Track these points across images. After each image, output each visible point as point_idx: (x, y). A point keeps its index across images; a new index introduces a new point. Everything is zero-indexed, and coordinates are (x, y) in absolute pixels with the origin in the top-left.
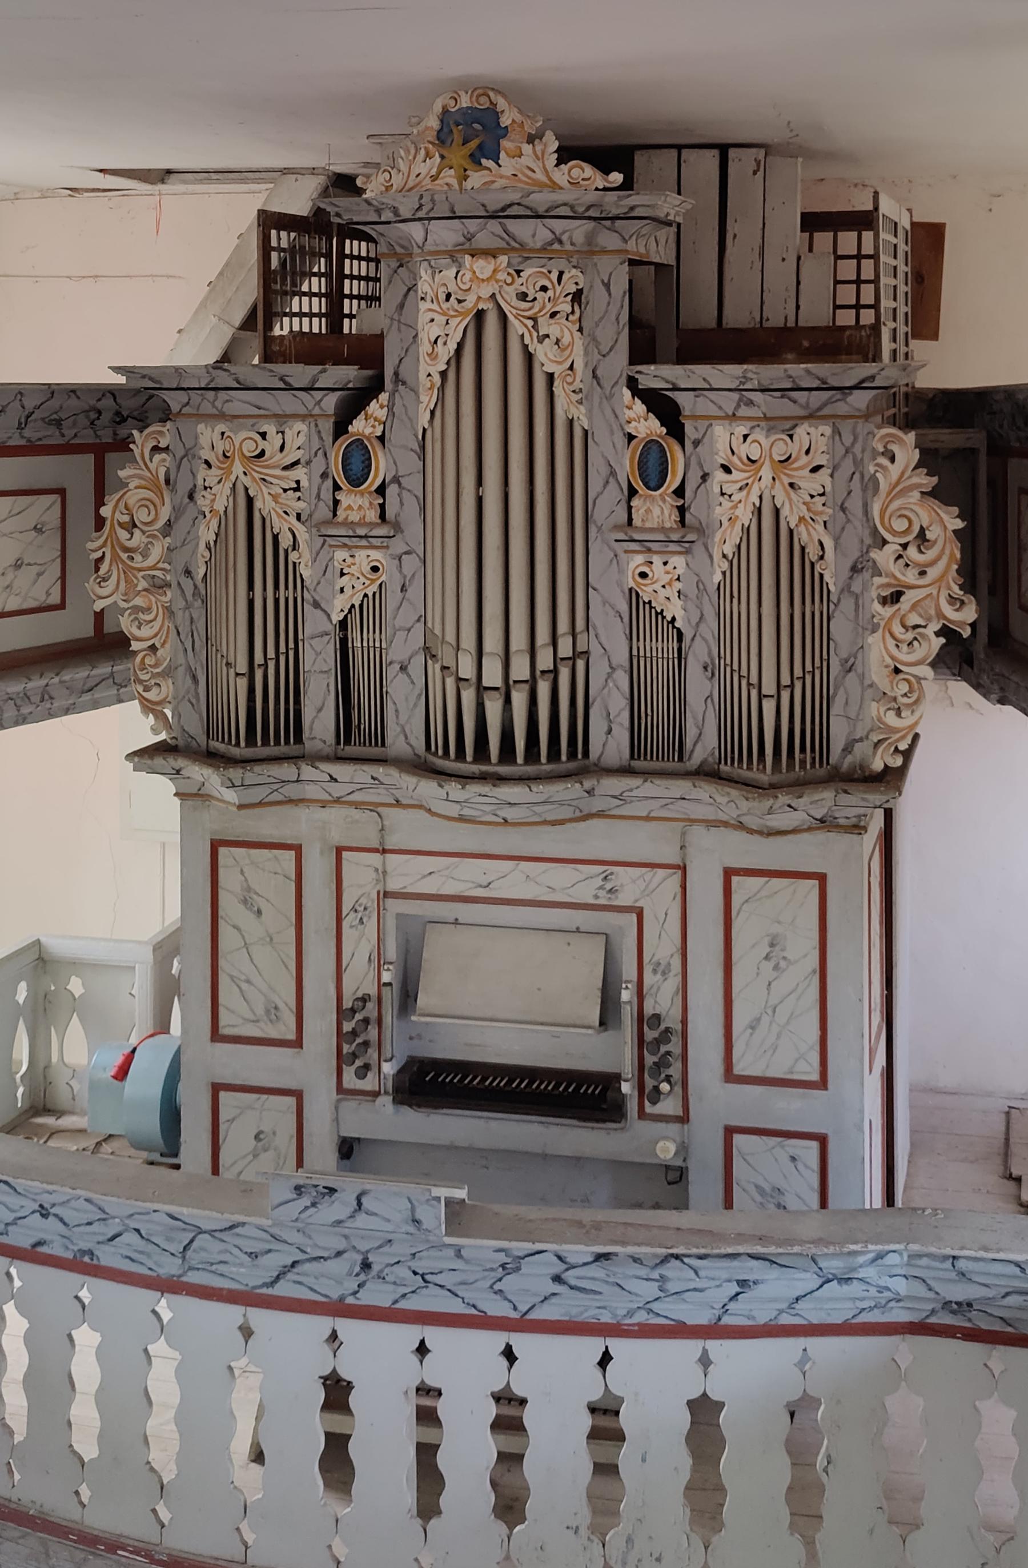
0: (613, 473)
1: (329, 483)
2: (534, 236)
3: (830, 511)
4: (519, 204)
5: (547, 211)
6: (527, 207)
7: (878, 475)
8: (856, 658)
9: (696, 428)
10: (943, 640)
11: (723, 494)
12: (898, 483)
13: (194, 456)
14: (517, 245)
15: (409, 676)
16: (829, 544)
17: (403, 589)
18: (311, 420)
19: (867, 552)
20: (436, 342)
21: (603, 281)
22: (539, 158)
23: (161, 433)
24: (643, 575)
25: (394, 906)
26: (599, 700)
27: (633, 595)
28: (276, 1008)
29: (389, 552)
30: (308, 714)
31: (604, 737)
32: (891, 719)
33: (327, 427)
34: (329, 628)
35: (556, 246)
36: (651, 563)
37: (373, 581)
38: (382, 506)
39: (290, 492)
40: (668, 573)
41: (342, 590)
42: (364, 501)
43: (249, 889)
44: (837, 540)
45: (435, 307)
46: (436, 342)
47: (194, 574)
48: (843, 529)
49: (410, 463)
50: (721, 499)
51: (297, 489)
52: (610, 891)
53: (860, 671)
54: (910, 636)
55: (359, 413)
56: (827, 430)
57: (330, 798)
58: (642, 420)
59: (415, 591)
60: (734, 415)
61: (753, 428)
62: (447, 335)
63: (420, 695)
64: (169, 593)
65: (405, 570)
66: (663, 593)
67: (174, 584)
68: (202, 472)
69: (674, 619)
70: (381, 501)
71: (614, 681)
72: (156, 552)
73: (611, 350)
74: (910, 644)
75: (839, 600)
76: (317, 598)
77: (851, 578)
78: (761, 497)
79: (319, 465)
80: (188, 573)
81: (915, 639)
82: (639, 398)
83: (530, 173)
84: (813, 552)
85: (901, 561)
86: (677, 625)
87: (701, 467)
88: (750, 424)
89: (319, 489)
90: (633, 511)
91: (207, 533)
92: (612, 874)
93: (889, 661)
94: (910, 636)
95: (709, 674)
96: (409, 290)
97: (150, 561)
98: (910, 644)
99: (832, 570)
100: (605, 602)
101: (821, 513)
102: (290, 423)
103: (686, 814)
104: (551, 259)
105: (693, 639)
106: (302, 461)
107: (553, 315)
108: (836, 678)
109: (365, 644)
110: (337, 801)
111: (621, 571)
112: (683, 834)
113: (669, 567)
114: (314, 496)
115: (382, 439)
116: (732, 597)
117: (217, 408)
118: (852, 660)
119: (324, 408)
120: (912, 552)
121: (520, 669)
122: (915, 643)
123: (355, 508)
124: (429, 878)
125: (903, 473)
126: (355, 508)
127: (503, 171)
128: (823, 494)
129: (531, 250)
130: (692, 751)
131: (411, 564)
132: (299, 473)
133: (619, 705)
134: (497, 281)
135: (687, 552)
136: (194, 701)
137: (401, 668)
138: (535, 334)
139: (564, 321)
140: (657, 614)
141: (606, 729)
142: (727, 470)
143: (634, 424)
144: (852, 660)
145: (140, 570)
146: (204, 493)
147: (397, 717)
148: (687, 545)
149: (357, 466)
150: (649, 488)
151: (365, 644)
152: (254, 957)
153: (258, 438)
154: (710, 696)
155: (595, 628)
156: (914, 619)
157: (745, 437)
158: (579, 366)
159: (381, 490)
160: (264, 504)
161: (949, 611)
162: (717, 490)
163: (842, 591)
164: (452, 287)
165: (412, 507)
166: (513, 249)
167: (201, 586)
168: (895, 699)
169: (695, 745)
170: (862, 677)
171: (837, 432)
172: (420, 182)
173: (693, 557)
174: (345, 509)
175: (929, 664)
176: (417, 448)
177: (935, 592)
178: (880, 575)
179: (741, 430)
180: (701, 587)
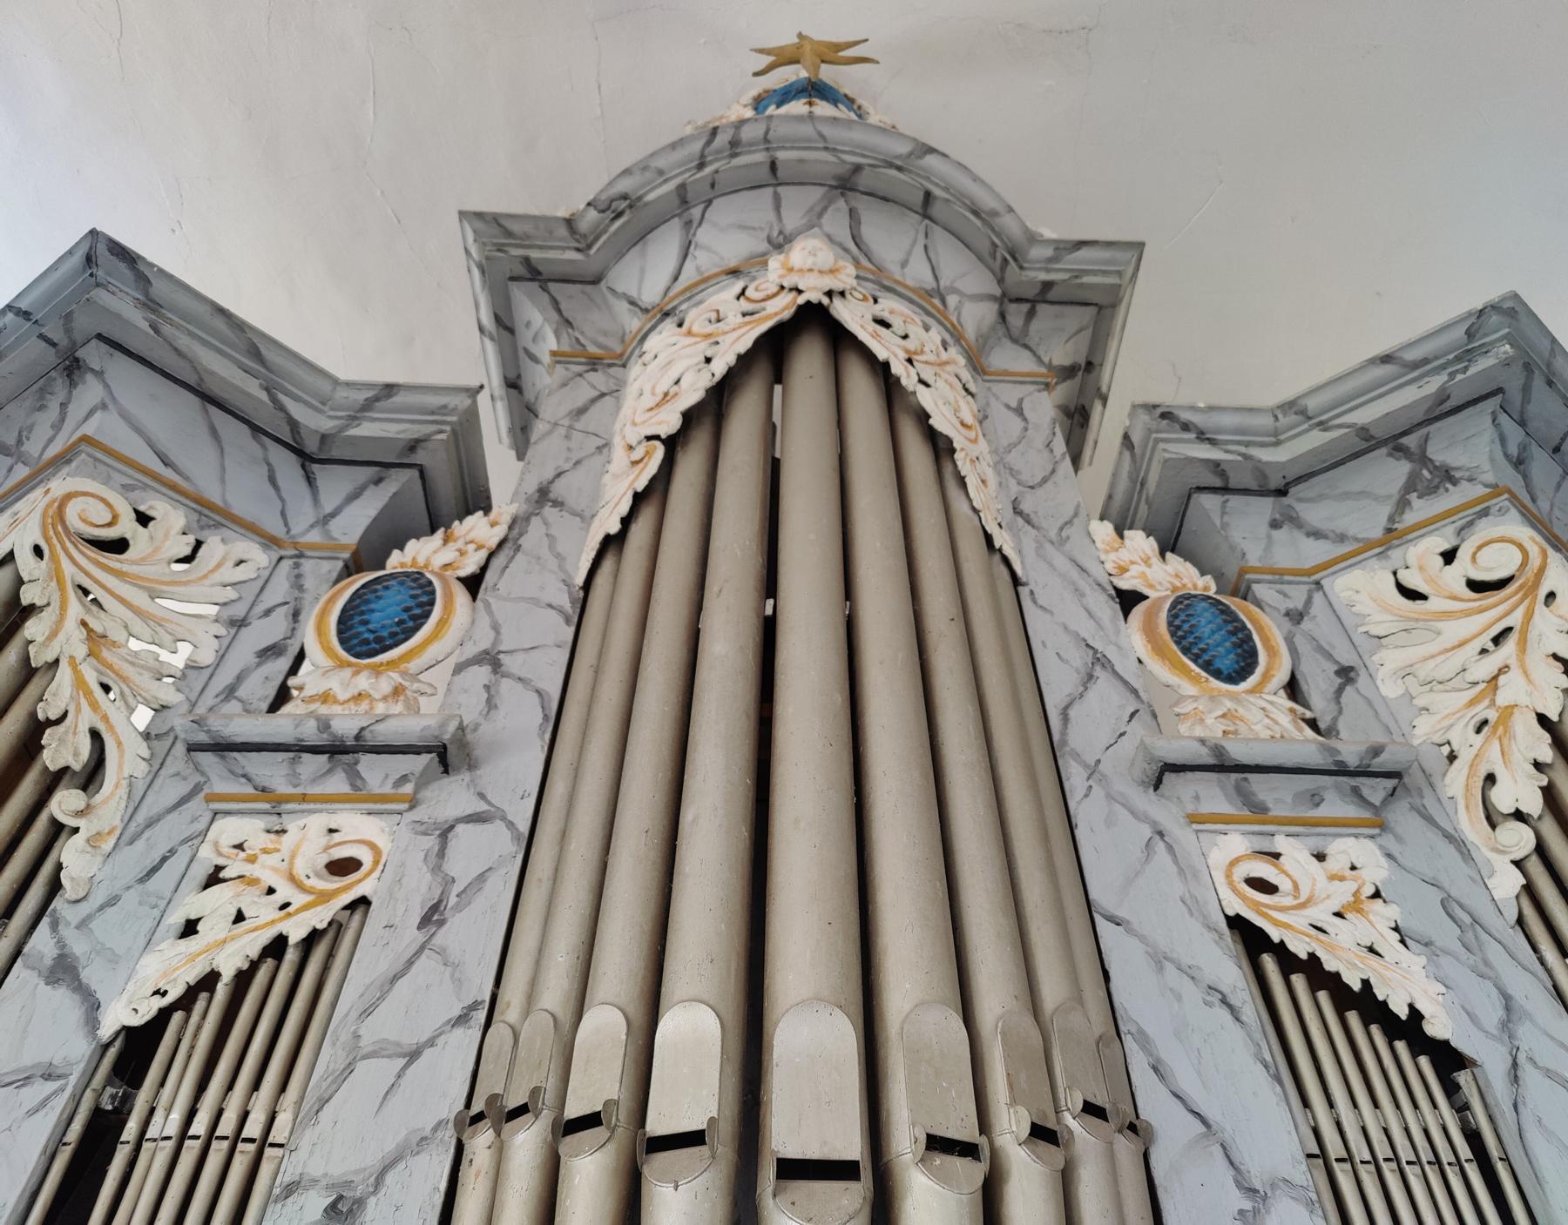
17: (432, 917)
36: (1277, 856)
37: (324, 897)
41: (190, 928)
60: (1389, 530)
65: (454, 865)
87: (1329, 656)
88: (1450, 530)
100: (1159, 960)
113: (1333, 864)
135: (1377, 824)
143: (1134, 570)
155: (1144, 1040)
173: (1399, 839)
176: (564, 601)
180: (1467, 920)
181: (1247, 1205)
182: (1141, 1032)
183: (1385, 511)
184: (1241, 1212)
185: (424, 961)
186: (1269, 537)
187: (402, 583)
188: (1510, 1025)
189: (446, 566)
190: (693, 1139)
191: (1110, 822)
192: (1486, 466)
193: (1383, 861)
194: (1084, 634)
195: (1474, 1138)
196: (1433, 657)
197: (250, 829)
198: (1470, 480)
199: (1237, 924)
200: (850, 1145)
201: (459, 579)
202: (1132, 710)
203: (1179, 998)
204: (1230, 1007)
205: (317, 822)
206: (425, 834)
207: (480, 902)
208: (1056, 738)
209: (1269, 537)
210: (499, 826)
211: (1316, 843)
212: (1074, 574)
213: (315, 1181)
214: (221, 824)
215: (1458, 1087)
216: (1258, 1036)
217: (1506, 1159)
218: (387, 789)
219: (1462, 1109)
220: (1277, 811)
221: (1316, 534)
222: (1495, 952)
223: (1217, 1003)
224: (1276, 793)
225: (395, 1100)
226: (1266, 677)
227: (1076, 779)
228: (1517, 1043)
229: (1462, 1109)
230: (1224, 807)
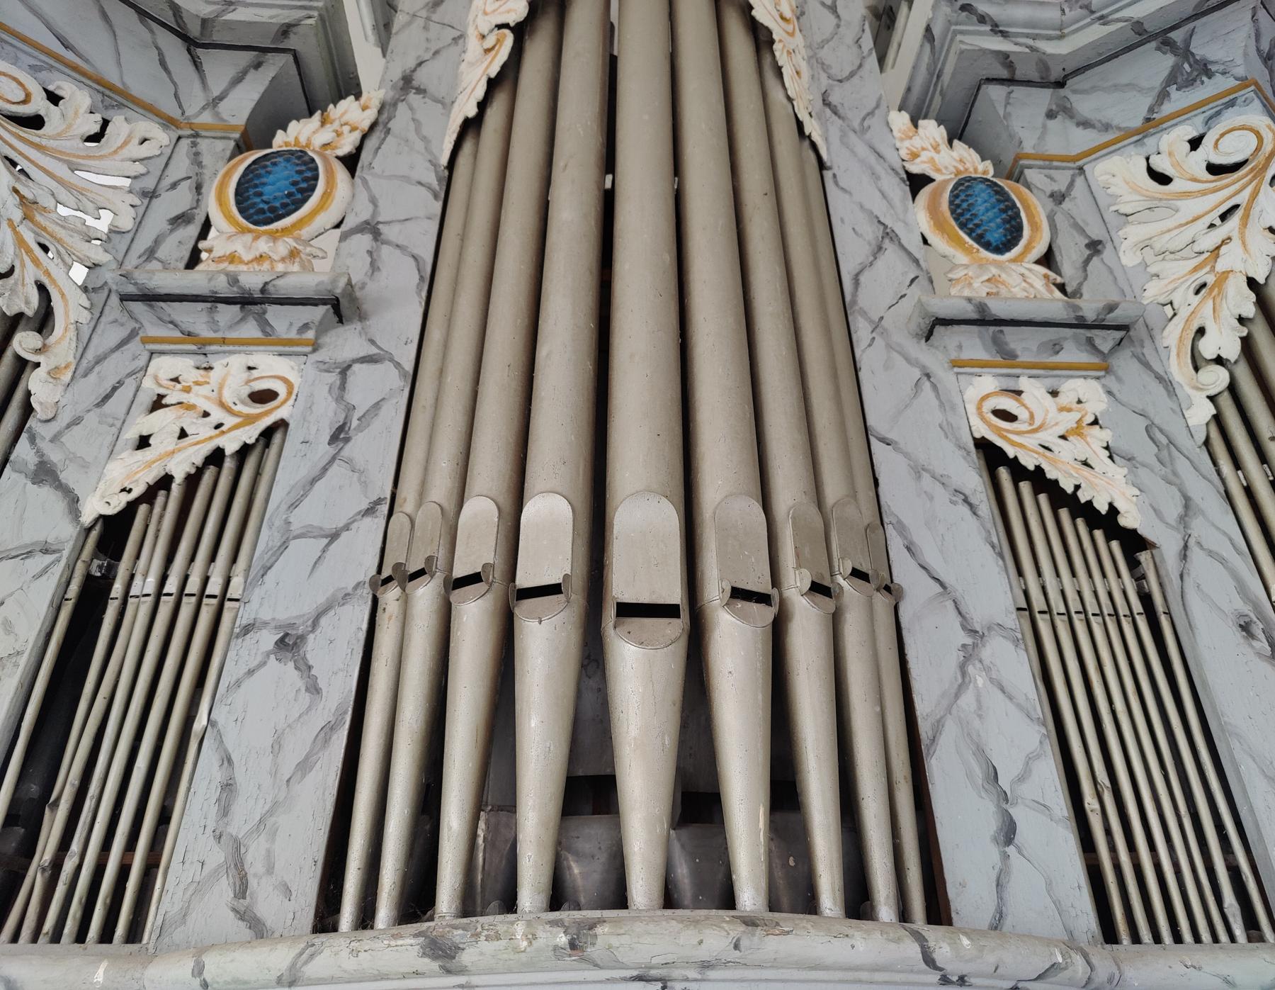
17: (340, 435)
27: (991, 455)
31: (994, 853)
34: (66, 533)
36: (1019, 393)
37: (250, 420)
41: (144, 442)
60: (1148, 120)
63: (330, 728)
87: (1082, 231)
88: (1200, 120)
100: (918, 471)
113: (1063, 399)
135: (1103, 368)
137: (282, 643)
143: (925, 156)
147: (225, 812)
155: (901, 529)
173: (1119, 379)
180: (1164, 441)
181: (969, 641)
182: (900, 522)
183: (1148, 100)
184: (964, 646)
185: (335, 469)
186: (1044, 126)
187: (288, 160)
188: (1186, 519)
189: (326, 146)
190: (554, 589)
191: (887, 366)
192: (1239, 61)
193: (1104, 397)
194: (876, 212)
195: (1146, 599)
196: (1169, 231)
197: (183, 366)
198: (1224, 73)
199: (983, 446)
200: (674, 594)
201: (338, 157)
202: (912, 276)
203: (931, 498)
204: (971, 506)
205: (237, 362)
206: (328, 371)
207: (377, 425)
208: (848, 298)
209: (1044, 126)
211: (1051, 383)
212: (872, 159)
213: (265, 624)
214: (157, 362)
215: (1139, 563)
216: (990, 525)
217: (1168, 613)
218: (293, 334)
219: (1139, 578)
220: (1024, 358)
221: (1085, 124)
222: (1182, 465)
223: (960, 501)
224: (1024, 343)
225: (322, 568)
226: (1028, 248)
227: (862, 332)
228: (1189, 532)
229: (1139, 578)
230: (982, 355)
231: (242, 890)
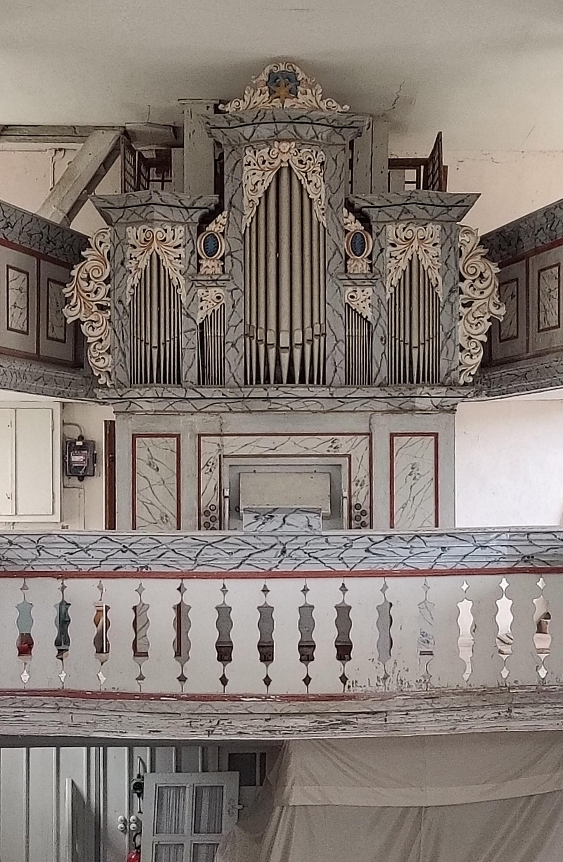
0: (338, 249)
1: (195, 256)
2: (307, 133)
3: (440, 264)
4: (305, 116)
5: (318, 120)
6: (309, 118)
7: (462, 248)
8: (452, 332)
9: (378, 228)
10: (490, 324)
11: (391, 257)
12: (470, 252)
13: (124, 244)
14: (299, 138)
15: (236, 349)
16: (440, 280)
17: (233, 306)
18: (186, 225)
19: (457, 284)
20: (256, 184)
21: (333, 158)
22: (315, 96)
23: (106, 233)
24: (352, 297)
25: (227, 462)
26: (330, 357)
28: (166, 516)
29: (227, 288)
30: (184, 369)
32: (468, 360)
33: (194, 229)
35: (316, 139)
37: (218, 303)
38: (223, 266)
39: (177, 260)
40: (364, 295)
41: (202, 308)
42: (215, 264)
43: (152, 458)
44: (443, 278)
45: (257, 167)
46: (256, 184)
47: (124, 302)
48: (446, 273)
49: (237, 245)
50: (390, 259)
51: (180, 258)
52: (335, 448)
53: (454, 338)
54: (476, 321)
55: (212, 221)
56: (440, 227)
57: (196, 410)
58: (353, 223)
59: (240, 308)
60: (398, 219)
61: (409, 224)
62: (263, 180)
64: (109, 312)
66: (362, 305)
67: (112, 308)
68: (130, 250)
69: (367, 317)
70: (223, 264)
71: (338, 347)
72: (102, 292)
73: (337, 191)
74: (476, 325)
75: (444, 305)
76: (189, 312)
77: (449, 295)
78: (412, 255)
79: (190, 247)
80: (120, 301)
81: (479, 323)
82: (352, 212)
83: (310, 102)
84: (434, 282)
85: (472, 288)
86: (368, 320)
89: (190, 259)
90: (348, 266)
91: (132, 280)
92: (336, 439)
93: (466, 333)
94: (476, 321)
95: (383, 342)
96: (237, 162)
97: (99, 297)
98: (476, 325)
99: (441, 292)
101: (437, 265)
102: (177, 226)
103: (372, 408)
104: (313, 145)
105: (376, 327)
106: (182, 245)
107: (314, 172)
108: (443, 342)
109: (213, 335)
110: (200, 411)
111: (341, 295)
112: (371, 418)
113: (365, 293)
114: (187, 262)
115: (223, 234)
116: (395, 304)
117: (142, 218)
118: (450, 334)
119: (193, 219)
120: (477, 283)
121: (298, 339)
122: (479, 325)
123: (210, 267)
124: (245, 447)
125: (473, 248)
126: (210, 267)
127: (299, 101)
128: (437, 257)
129: (305, 140)
130: (375, 379)
131: (237, 294)
132: (181, 250)
133: (340, 358)
134: (290, 153)
136: (123, 366)
138: (306, 180)
139: (318, 175)
140: (358, 315)
141: (334, 370)
142: (394, 245)
143: (349, 225)
144: (450, 334)
145: (93, 301)
146: (130, 261)
147: (230, 369)
148: (374, 281)
149: (211, 246)
150: (356, 255)
151: (213, 335)
152: (155, 492)
153: (164, 231)
154: (384, 353)
155: (329, 323)
156: (478, 314)
157: (404, 229)
158: (323, 197)
159: (222, 259)
160: (166, 263)
161: (494, 310)
162: (388, 255)
163: (445, 302)
164: (266, 157)
165: (238, 267)
166: (297, 139)
167: (128, 308)
168: (469, 351)
169: (377, 376)
170: (454, 341)
171: (443, 228)
172: (256, 106)
174: (205, 268)
175: (486, 334)
177: (487, 302)
178: (462, 293)
179: (402, 225)
180: (380, 301)
185: (234, 313)
207: (239, 303)
210: (239, 290)
231: (235, 379)
